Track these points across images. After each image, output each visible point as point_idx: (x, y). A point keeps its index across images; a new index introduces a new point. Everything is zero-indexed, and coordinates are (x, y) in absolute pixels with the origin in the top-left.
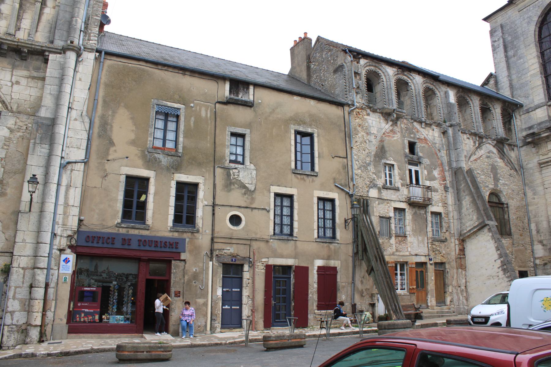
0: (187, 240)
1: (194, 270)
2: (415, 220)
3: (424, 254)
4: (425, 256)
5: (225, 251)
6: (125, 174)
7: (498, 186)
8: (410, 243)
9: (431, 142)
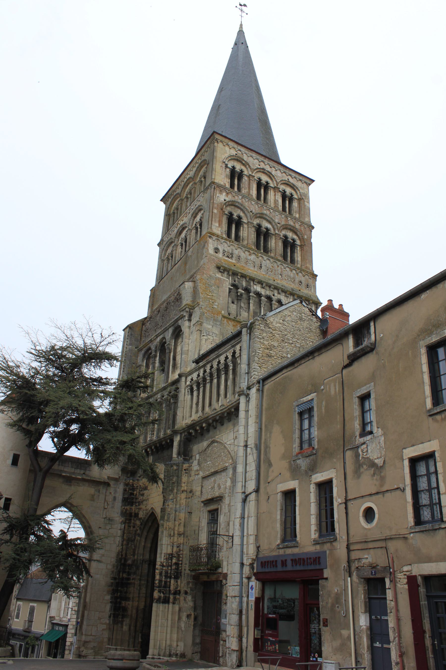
0: (328, 552)
1: (336, 591)
5: (364, 561)
6: (280, 492)
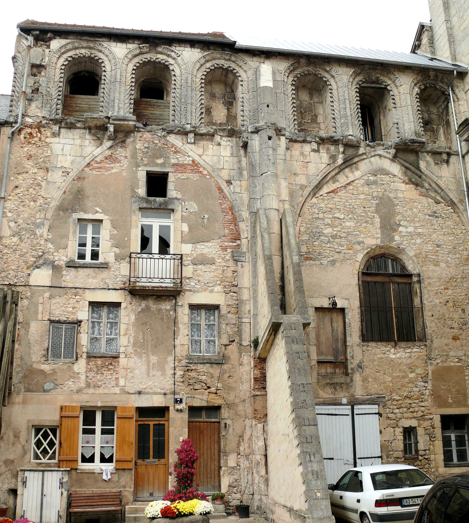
2: (145, 324)
3: (163, 391)
4: (165, 394)
7: (392, 239)
8: (126, 369)
9: (210, 169)
